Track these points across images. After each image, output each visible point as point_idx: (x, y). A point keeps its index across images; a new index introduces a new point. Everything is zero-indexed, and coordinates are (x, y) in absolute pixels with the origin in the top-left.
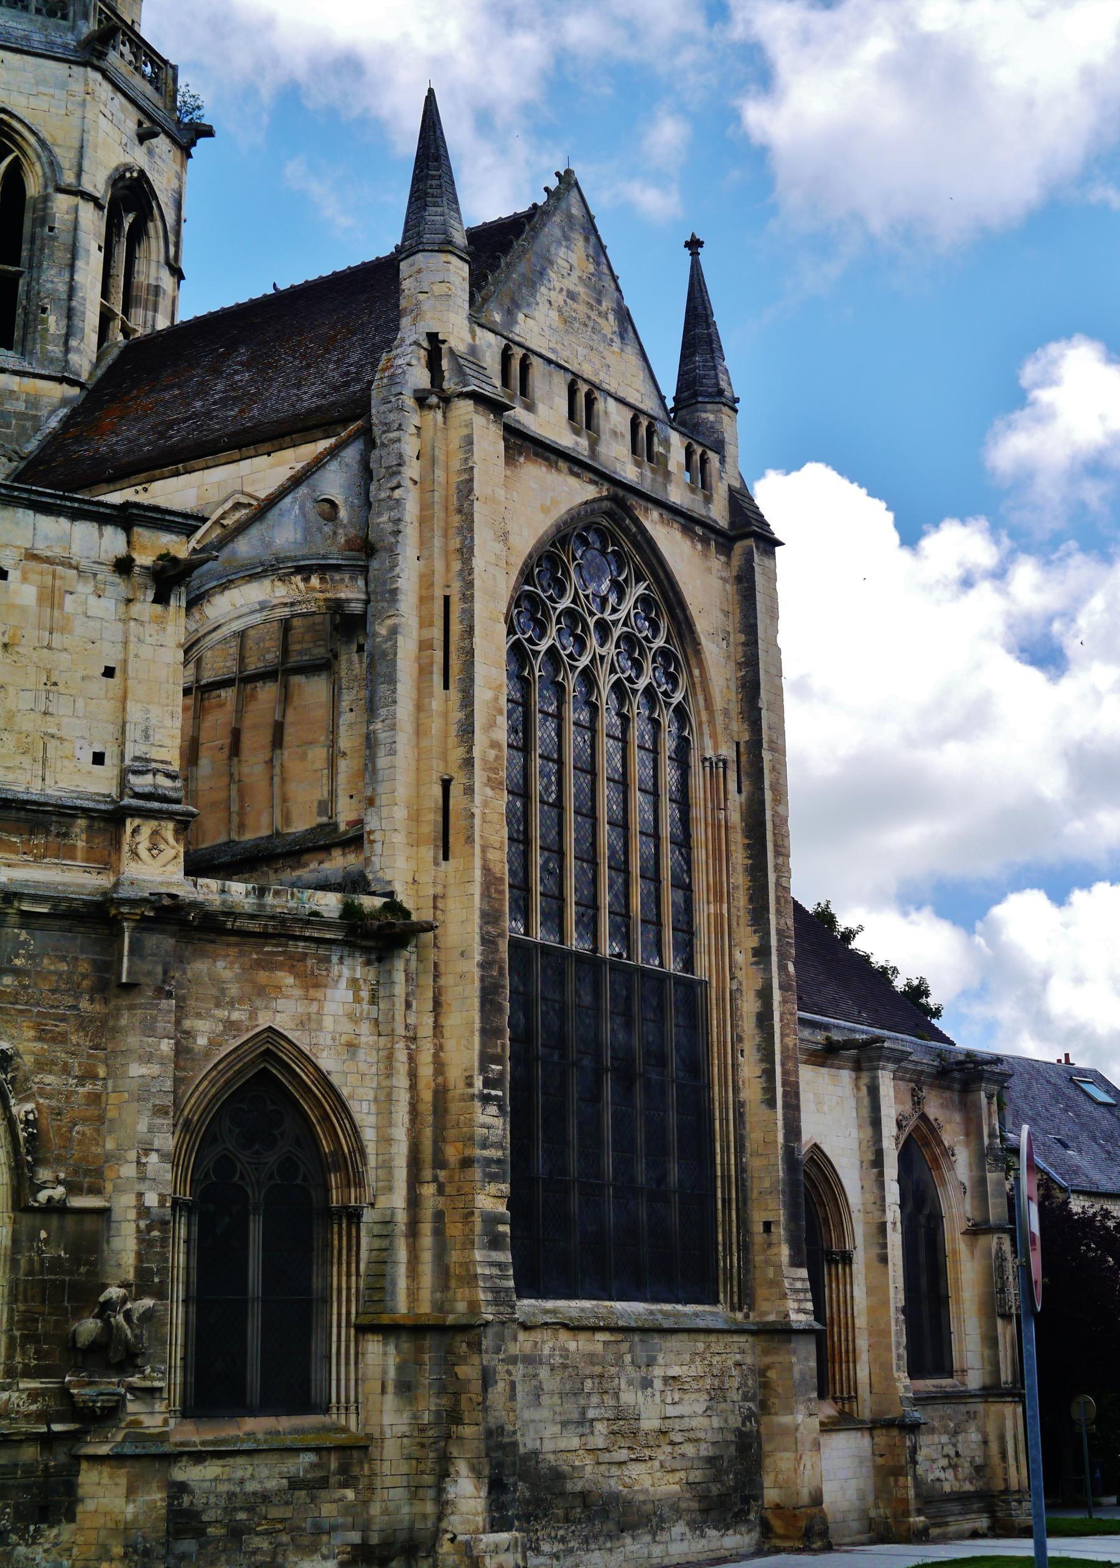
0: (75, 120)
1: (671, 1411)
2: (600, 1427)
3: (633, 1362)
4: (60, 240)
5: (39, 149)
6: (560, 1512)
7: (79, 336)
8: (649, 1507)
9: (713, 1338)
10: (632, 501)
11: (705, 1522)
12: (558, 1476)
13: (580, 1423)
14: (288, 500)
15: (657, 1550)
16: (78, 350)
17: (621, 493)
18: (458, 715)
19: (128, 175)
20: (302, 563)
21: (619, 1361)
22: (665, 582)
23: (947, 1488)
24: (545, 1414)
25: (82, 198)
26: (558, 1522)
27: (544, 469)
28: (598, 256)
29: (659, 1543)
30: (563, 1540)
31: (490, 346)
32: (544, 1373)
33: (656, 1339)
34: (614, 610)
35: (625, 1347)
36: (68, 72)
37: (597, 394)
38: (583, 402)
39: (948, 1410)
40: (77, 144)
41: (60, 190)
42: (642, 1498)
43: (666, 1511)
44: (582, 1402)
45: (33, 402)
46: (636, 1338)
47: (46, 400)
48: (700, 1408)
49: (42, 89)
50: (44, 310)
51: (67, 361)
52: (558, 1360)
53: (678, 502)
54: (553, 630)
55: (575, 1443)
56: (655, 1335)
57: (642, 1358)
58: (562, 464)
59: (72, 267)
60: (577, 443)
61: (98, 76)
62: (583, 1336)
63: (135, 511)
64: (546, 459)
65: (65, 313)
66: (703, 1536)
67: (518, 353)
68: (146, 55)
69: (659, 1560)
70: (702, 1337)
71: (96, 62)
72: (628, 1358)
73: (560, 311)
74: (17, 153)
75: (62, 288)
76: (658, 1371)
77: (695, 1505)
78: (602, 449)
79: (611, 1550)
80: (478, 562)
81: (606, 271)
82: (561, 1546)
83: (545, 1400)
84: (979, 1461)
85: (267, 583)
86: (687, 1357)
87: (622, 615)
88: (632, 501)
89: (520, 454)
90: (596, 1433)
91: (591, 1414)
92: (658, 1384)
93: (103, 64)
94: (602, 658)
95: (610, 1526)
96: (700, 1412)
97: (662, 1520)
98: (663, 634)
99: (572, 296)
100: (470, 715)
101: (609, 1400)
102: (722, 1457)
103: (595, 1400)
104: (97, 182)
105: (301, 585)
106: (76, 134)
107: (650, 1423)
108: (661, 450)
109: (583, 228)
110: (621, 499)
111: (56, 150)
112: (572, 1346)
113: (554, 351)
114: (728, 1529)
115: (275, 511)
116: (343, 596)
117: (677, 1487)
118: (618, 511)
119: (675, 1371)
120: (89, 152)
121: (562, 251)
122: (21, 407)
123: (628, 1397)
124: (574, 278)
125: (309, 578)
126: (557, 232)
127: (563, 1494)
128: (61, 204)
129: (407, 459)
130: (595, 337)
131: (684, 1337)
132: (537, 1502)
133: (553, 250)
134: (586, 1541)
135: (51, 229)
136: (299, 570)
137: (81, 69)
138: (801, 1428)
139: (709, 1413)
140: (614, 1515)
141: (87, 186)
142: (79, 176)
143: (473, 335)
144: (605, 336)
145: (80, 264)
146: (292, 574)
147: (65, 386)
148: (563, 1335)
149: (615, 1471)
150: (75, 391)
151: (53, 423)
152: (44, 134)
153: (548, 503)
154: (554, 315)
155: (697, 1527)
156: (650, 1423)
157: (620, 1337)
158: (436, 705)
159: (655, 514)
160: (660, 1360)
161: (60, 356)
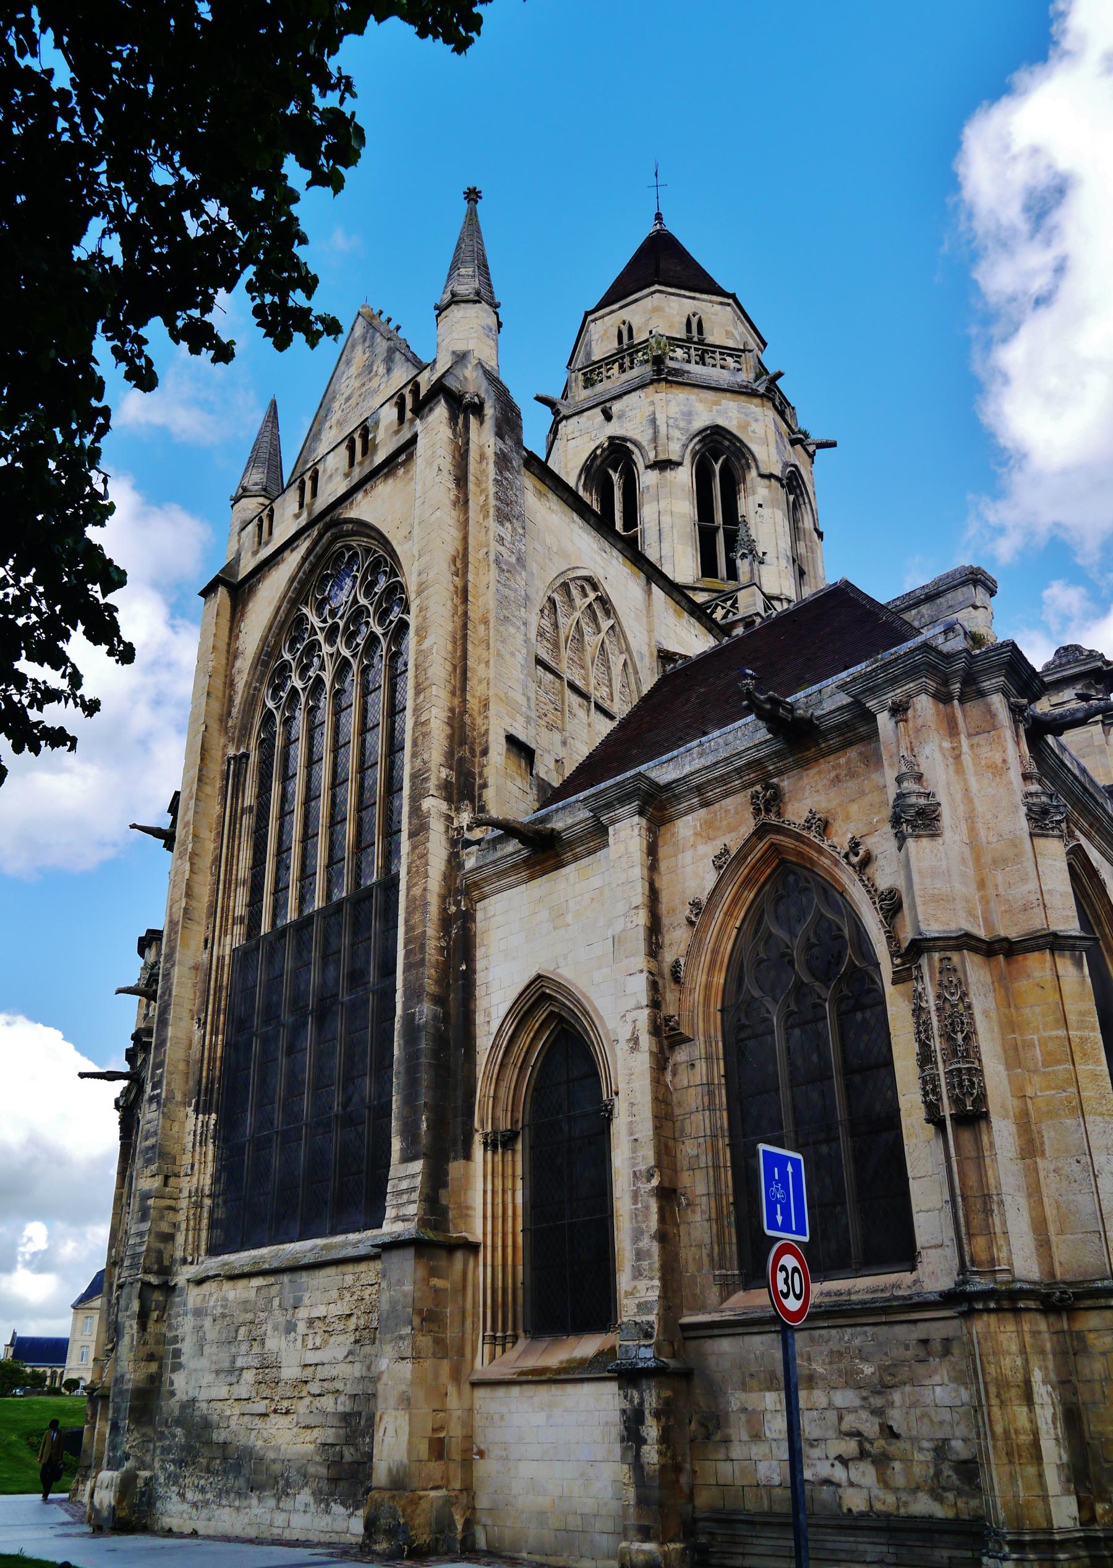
1: (311, 1357)
2: (249, 1376)
3: (280, 1306)
6: (204, 1461)
8: (277, 1468)
9: (362, 1267)
11: (332, 1494)
12: (207, 1425)
13: (231, 1371)
15: (280, 1519)
19: (599, 452)
21: (268, 1308)
23: (855, 1501)
24: (204, 1363)
26: (201, 1471)
29: (282, 1510)
30: (202, 1490)
32: (208, 1322)
33: (304, 1277)
35: (274, 1290)
39: (855, 1338)
42: (271, 1455)
43: (294, 1475)
44: (234, 1350)
46: (285, 1278)
48: (341, 1353)
52: (219, 1310)
55: (223, 1392)
56: (304, 1274)
57: (289, 1302)
62: (241, 1284)
66: (327, 1511)
69: (279, 1531)
70: (350, 1268)
72: (276, 1302)
76: (303, 1313)
77: (323, 1471)
79: (238, 1509)
82: (200, 1497)
83: (207, 1350)
84: (960, 1449)
86: (334, 1294)
90: (242, 1381)
91: (239, 1363)
92: (302, 1327)
95: (241, 1482)
96: (341, 1358)
97: (288, 1484)
101: (256, 1349)
102: (360, 1413)
103: (244, 1348)
107: (290, 1372)
112: (231, 1295)
114: (357, 1508)
117: (312, 1447)
119: (320, 1311)
123: (273, 1343)
127: (209, 1443)
131: (331, 1271)
132: (188, 1448)
134: (219, 1496)
138: (385, 1378)
139: (350, 1358)
140: (245, 1471)
148: (227, 1285)
149: (258, 1422)
155: (323, 1498)
156: (290, 1372)
157: (271, 1280)
160: (306, 1301)
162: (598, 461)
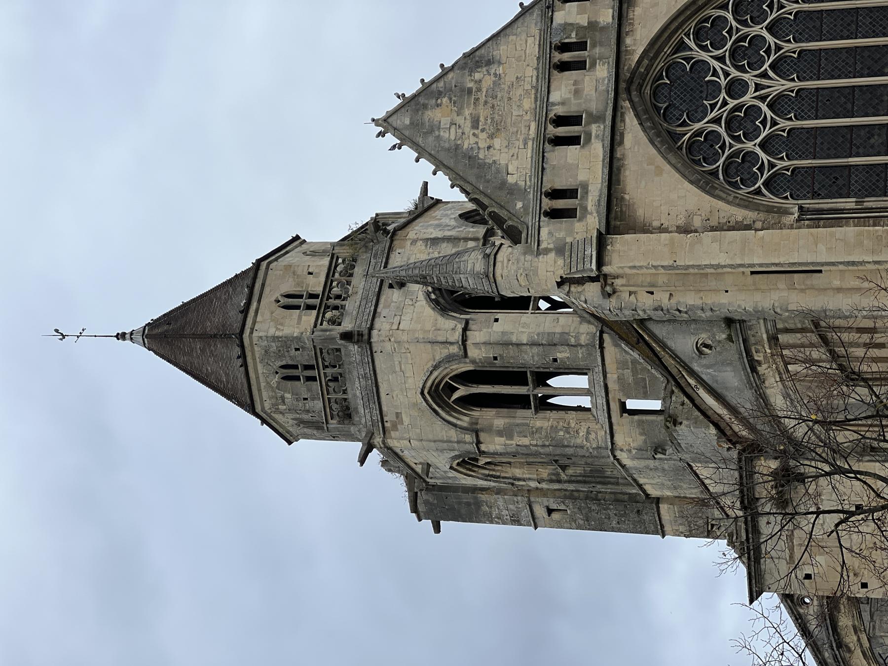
0: (412, 348)
4: (501, 353)
5: (441, 369)
7: (567, 337)
10: (626, 74)
14: (704, 377)
16: (577, 337)
17: (623, 85)
18: (841, 267)
19: (433, 296)
20: (749, 370)
22: (680, 20)
25: (466, 340)
27: (627, 173)
28: (432, 92)
31: (550, 233)
34: (715, 73)
36: (378, 353)
37: (551, 115)
38: (563, 130)
40: (429, 346)
41: (466, 355)
45: (622, 365)
47: (618, 356)
49: (398, 369)
50: (555, 360)
51: (587, 345)
53: (611, 11)
54: (749, 146)
58: (618, 155)
59: (518, 345)
60: (597, 137)
61: (375, 333)
63: (746, 501)
64: (619, 170)
65: (553, 347)
67: (547, 204)
68: (333, 276)
71: (366, 337)
73: (491, 137)
74: (447, 379)
75: (535, 350)
78: (594, 106)
80: (723, 259)
81: (441, 84)
85: (769, 392)
87: (716, 64)
88: (626, 74)
89: (623, 198)
93: (366, 332)
94: (758, 87)
98: (721, 13)
99: (475, 123)
100: (841, 263)
104: (449, 327)
105: (764, 366)
106: (422, 345)
108: (573, 35)
109: (418, 111)
110: (625, 84)
111: (438, 358)
113: (525, 144)
115: (714, 385)
116: (765, 336)
118: (637, 81)
120: (431, 336)
121: (444, 135)
122: (628, 373)
124: (459, 120)
125: (757, 361)
126: (431, 139)
128: (473, 352)
129: (656, 304)
130: (499, 96)
133: (447, 145)
135: (495, 358)
136: (754, 370)
137: (374, 345)
141: (457, 336)
142: (451, 343)
143: (547, 251)
144: (494, 83)
145: (514, 339)
146: (757, 373)
147: (605, 345)
150: (605, 336)
151: (635, 355)
152: (429, 366)
153: (653, 167)
154: (497, 143)
158: (837, 283)
159: (628, 41)
161: (584, 349)
162: (441, 300)
